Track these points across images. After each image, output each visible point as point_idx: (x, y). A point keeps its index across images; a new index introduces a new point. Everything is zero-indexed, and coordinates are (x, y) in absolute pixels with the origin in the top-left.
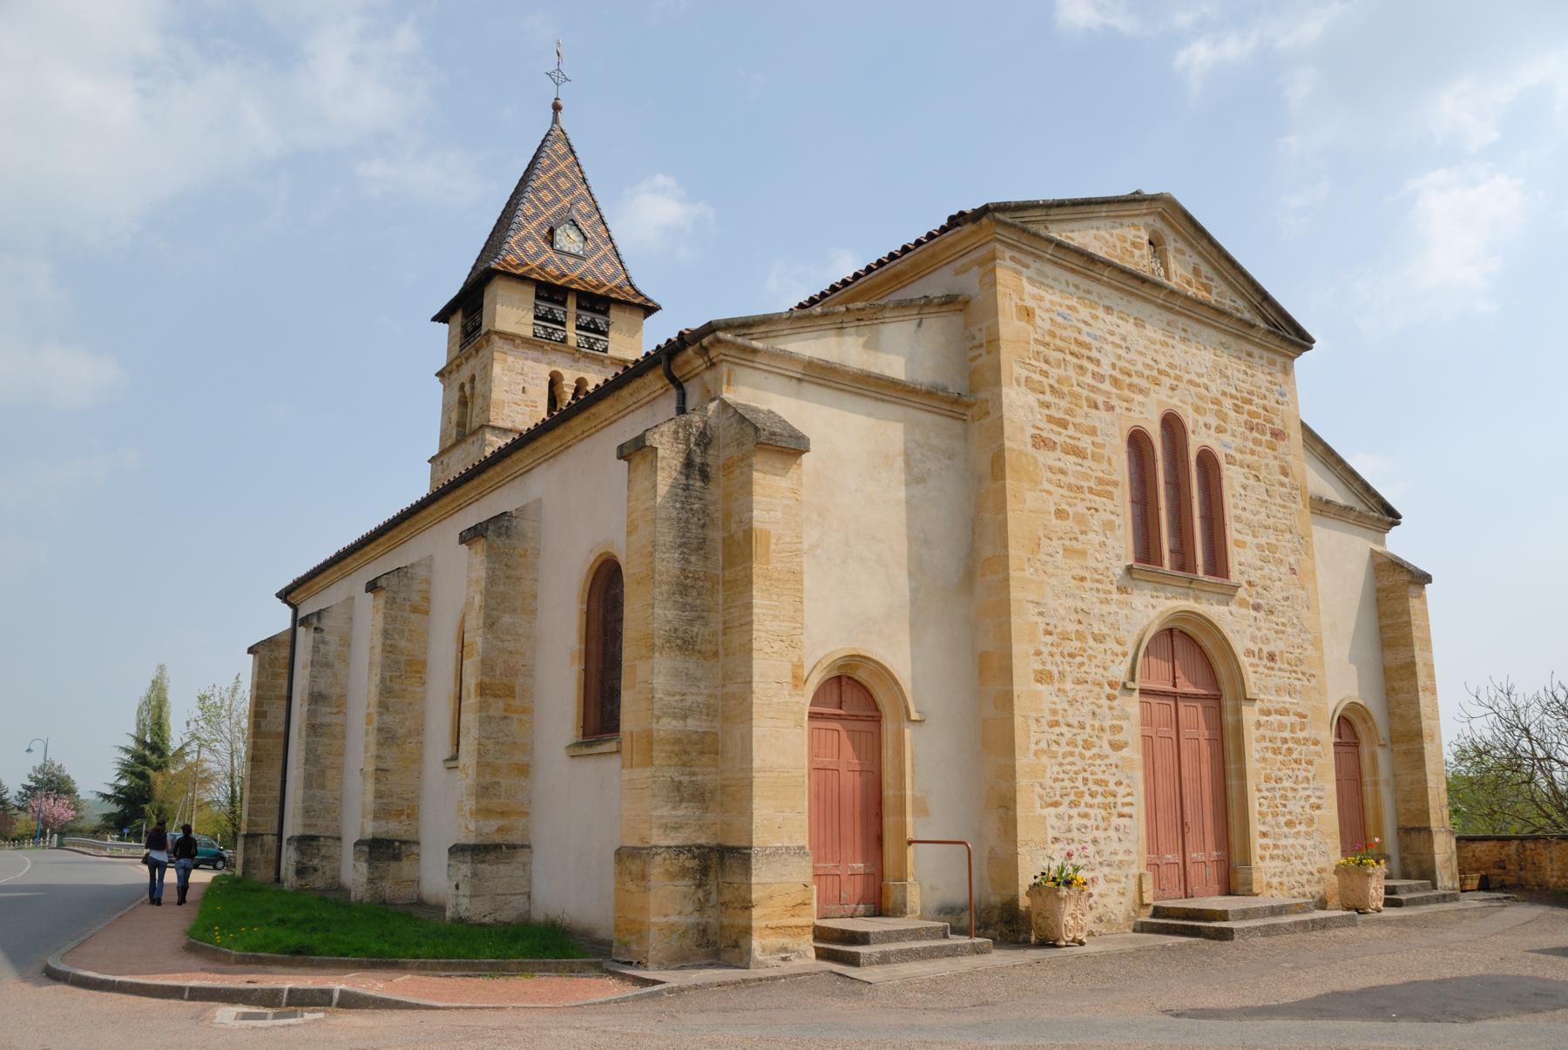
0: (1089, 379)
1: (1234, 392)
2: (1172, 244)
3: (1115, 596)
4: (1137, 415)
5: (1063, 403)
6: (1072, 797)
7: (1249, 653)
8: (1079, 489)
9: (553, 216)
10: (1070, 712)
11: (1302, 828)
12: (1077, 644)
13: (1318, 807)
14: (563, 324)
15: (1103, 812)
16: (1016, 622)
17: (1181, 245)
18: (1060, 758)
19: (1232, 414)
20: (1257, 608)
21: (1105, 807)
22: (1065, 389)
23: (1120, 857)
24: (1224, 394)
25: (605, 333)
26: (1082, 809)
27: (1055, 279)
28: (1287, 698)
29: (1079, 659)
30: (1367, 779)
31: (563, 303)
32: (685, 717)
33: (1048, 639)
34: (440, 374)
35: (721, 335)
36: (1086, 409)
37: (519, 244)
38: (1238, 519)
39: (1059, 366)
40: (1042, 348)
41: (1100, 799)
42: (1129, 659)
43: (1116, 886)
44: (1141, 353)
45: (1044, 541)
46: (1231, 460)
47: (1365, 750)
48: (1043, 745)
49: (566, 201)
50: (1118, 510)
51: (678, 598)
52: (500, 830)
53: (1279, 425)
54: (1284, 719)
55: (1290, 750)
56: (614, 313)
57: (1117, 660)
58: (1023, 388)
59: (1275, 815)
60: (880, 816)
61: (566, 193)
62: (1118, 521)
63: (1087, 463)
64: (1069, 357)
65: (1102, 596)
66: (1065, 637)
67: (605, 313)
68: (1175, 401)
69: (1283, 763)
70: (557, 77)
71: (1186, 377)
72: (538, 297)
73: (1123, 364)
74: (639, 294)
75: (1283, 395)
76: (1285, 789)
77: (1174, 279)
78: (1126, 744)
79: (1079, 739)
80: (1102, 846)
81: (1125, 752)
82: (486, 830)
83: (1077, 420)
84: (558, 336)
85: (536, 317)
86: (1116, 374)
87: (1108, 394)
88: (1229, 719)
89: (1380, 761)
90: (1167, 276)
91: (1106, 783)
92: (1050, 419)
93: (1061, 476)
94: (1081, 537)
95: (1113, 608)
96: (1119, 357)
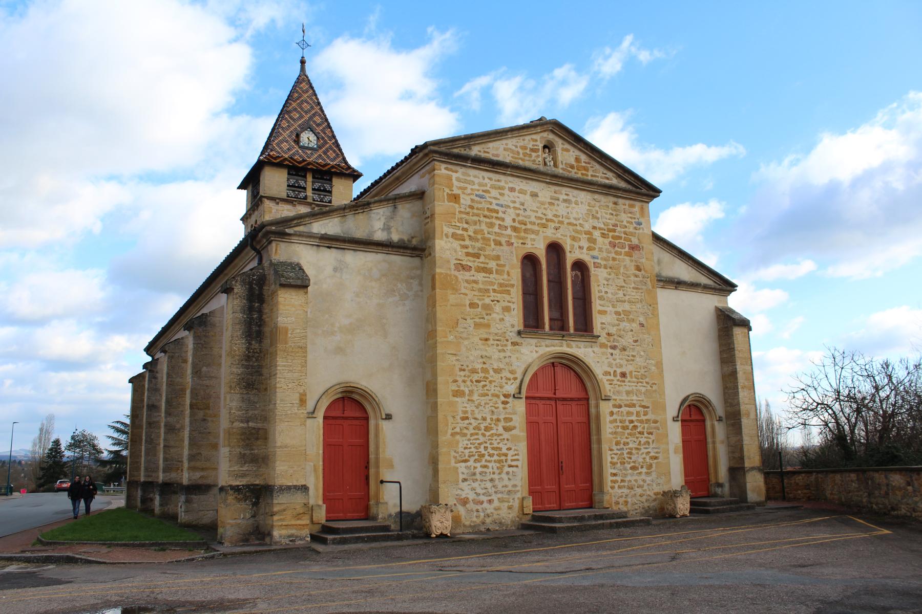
0: (496, 229)
1: (603, 226)
2: (560, 145)
3: (510, 347)
4: (529, 246)
5: (478, 245)
6: (476, 457)
7: (607, 373)
8: (487, 291)
9: (299, 126)
10: (476, 411)
11: (644, 470)
12: (483, 375)
13: (656, 458)
14: (305, 188)
15: (498, 465)
16: (440, 364)
17: (567, 146)
18: (469, 436)
19: (600, 240)
20: (614, 348)
21: (500, 461)
22: (479, 237)
23: (510, 488)
24: (594, 228)
25: (330, 192)
26: (483, 463)
27: (475, 177)
28: (635, 398)
29: (483, 383)
30: (709, 440)
31: (305, 177)
32: (248, 422)
33: (462, 373)
34: (242, 219)
35: (268, 228)
36: (493, 246)
37: (278, 144)
38: (601, 298)
39: (475, 223)
40: (464, 216)
41: (496, 458)
42: (518, 381)
43: (506, 504)
44: (534, 211)
45: (461, 321)
46: (597, 266)
47: (708, 423)
48: (458, 430)
49: (307, 117)
50: (513, 300)
51: (244, 362)
52: (202, 477)
53: (635, 241)
54: (631, 409)
55: (635, 427)
56: (335, 181)
57: (510, 383)
58: (451, 239)
59: (623, 463)
60: (367, 467)
61: (306, 112)
62: (512, 306)
63: (494, 276)
64: (482, 219)
65: (500, 348)
66: (474, 371)
67: (331, 180)
68: (559, 235)
69: (629, 434)
70: (304, 44)
71: (566, 221)
72: (289, 174)
73: (521, 218)
74: (349, 167)
75: (640, 224)
76: (631, 449)
77: (561, 166)
78: (514, 428)
79: (482, 426)
80: (497, 482)
81: (513, 432)
82: (194, 478)
83: (487, 253)
84: (302, 195)
85: (288, 186)
86: (516, 225)
87: (510, 236)
88: (593, 410)
89: (718, 432)
90: (555, 165)
91: (500, 449)
92: (468, 254)
93: (475, 285)
94: (486, 317)
95: (508, 354)
96: (518, 215)
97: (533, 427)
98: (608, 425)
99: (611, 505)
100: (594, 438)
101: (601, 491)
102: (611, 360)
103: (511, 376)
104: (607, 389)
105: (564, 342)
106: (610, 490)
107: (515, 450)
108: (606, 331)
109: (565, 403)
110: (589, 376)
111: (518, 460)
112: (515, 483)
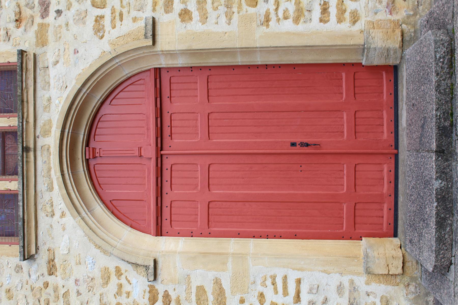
7: (99, 29)
42: (124, 266)
57: (127, 288)
78: (217, 282)
81: (226, 285)
88: (181, 62)
97: (214, 222)
98: (210, 27)
99: (398, 24)
100: (240, 60)
101: (363, 49)
102: (69, 15)
103: (114, 280)
104: (125, 32)
105: (40, 143)
106: (360, 25)
107: (264, 284)
108: (12, 26)
109: (166, 131)
110: (108, 75)
111: (285, 279)
112: (333, 288)
